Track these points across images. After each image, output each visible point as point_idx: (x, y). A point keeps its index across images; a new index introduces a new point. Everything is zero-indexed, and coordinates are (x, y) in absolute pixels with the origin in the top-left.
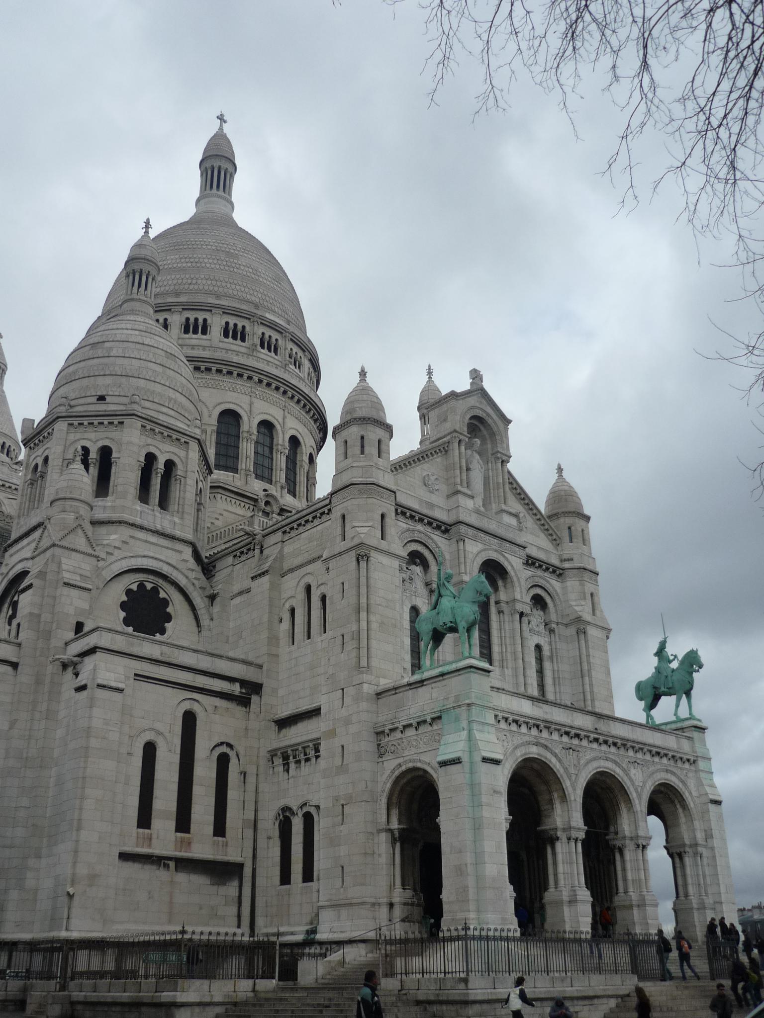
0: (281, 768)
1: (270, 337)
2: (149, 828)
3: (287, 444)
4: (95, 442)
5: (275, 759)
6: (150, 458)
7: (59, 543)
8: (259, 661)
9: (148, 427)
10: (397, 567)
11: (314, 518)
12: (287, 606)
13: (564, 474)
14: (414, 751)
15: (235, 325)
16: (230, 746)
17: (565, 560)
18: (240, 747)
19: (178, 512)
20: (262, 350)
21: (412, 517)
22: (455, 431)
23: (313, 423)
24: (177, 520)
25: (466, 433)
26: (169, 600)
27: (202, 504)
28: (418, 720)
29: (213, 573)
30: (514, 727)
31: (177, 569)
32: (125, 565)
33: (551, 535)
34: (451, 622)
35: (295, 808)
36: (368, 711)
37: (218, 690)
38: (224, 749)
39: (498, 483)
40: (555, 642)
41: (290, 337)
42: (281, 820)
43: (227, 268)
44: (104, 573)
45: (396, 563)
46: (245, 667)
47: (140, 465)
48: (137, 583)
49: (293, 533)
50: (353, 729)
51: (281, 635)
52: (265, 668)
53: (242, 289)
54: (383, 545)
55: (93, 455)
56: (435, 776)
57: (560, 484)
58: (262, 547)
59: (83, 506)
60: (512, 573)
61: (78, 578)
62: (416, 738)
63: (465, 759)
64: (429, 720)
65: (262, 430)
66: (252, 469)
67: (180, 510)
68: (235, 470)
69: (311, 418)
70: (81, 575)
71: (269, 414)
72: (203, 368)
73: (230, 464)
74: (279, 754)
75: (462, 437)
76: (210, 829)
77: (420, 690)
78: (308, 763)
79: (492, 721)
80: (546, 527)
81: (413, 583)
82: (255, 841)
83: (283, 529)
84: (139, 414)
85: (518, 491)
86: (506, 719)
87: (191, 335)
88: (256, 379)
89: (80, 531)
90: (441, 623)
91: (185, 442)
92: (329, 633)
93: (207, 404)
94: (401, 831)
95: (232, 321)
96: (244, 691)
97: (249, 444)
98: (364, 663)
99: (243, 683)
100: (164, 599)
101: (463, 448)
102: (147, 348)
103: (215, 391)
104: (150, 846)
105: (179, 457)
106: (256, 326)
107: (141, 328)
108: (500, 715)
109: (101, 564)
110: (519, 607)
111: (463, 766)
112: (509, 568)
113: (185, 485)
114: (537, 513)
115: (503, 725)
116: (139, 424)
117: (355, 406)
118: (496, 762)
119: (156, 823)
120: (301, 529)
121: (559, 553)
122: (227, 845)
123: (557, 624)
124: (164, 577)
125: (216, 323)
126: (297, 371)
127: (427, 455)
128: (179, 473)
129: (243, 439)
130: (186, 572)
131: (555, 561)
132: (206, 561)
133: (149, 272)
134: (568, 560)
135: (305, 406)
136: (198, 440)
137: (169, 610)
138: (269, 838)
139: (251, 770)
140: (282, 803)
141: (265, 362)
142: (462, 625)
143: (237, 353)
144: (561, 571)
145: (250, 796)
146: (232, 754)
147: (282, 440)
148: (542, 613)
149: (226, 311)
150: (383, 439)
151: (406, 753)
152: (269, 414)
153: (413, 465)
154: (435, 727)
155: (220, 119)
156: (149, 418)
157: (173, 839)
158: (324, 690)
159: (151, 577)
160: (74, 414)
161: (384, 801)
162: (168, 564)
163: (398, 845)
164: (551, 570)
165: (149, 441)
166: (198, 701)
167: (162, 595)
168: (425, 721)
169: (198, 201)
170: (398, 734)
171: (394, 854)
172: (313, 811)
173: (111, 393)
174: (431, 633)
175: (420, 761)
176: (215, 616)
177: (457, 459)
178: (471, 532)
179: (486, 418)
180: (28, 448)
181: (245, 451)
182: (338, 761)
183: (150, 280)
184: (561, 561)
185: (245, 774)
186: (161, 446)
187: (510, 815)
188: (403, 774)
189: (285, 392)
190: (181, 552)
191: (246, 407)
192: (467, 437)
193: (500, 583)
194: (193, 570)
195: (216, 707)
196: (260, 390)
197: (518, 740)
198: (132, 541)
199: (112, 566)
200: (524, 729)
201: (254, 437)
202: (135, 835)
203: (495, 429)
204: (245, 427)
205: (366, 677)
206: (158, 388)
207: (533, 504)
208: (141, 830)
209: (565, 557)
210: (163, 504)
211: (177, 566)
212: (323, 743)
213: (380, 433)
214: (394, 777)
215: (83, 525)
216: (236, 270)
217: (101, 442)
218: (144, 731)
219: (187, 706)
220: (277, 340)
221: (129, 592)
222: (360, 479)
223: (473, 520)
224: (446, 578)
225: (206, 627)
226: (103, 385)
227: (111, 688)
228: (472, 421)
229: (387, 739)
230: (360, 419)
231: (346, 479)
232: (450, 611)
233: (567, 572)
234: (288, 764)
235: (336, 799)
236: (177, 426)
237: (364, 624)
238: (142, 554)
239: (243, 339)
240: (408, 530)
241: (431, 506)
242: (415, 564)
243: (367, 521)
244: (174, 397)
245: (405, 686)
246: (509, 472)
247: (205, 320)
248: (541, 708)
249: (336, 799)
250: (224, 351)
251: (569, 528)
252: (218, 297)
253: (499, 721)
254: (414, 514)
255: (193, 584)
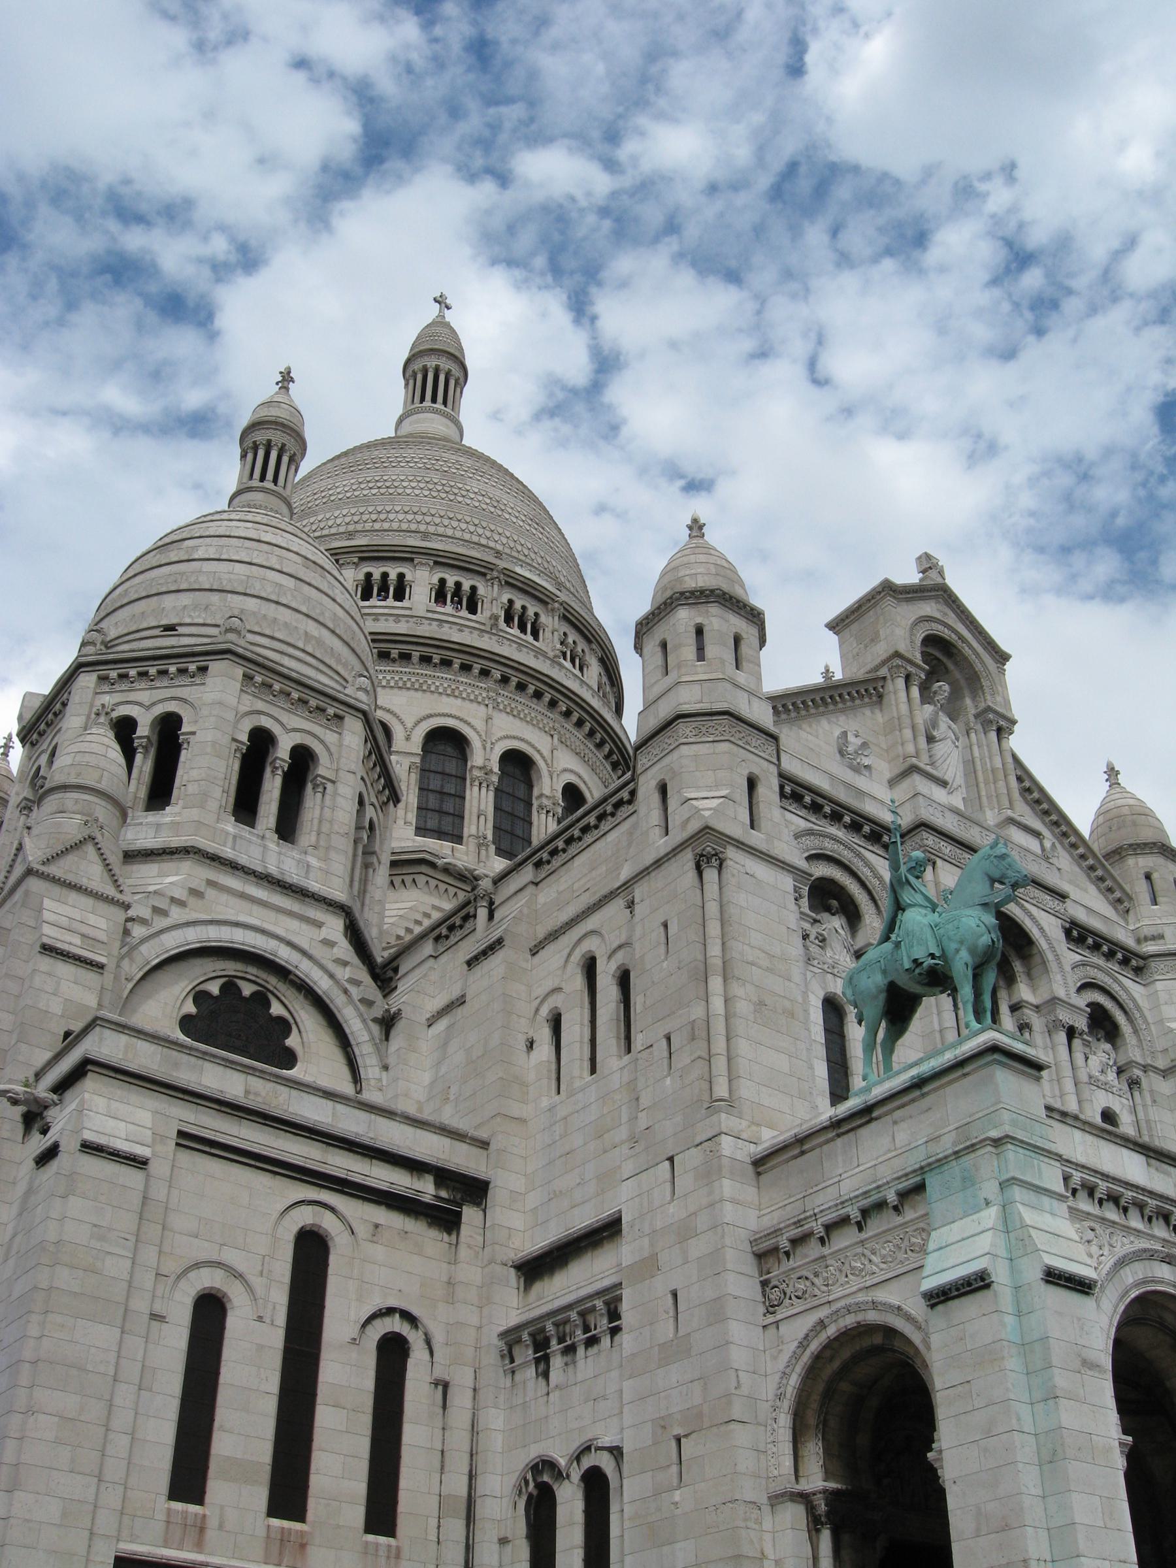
0: (531, 1372)
1: (524, 608)
2: (200, 1501)
3: (559, 795)
4: (148, 708)
5: (517, 1351)
6: (261, 741)
7: (42, 868)
8: (483, 1134)
9: (258, 679)
10: (791, 889)
11: (601, 818)
12: (545, 1011)
13: (1121, 779)
14: (855, 1283)
15: (458, 585)
16: (409, 1317)
17: (1146, 939)
18: (435, 1321)
19: (315, 847)
20: (508, 630)
21: (816, 808)
22: (897, 654)
23: (609, 768)
24: (313, 861)
25: (921, 663)
26: (291, 1021)
27: (374, 853)
28: (865, 1203)
29: (393, 985)
30: (1112, 1214)
31: (310, 957)
32: (193, 937)
33: (1110, 890)
34: (932, 956)
35: (562, 1462)
36: (734, 1201)
37: (383, 1186)
38: (395, 1324)
39: (993, 771)
40: (1145, 1106)
41: (562, 610)
42: (530, 1496)
43: (444, 495)
44: (144, 948)
45: (787, 882)
46: (446, 1141)
47: (234, 745)
48: (222, 981)
49: (556, 862)
50: (698, 1248)
51: (531, 1077)
52: (493, 1147)
53: (472, 528)
54: (756, 839)
55: (143, 730)
56: (916, 1338)
57: (1117, 796)
58: (491, 903)
59: (103, 803)
60: (1043, 944)
61: (77, 940)
62: (860, 1250)
63: (1000, 1275)
64: (892, 1197)
65: (510, 769)
66: (490, 837)
67: (322, 843)
68: (458, 838)
69: (607, 757)
70: (83, 936)
71: (522, 740)
72: (394, 654)
73: (448, 828)
74: (525, 1336)
75: (911, 669)
76: (357, 1515)
77: (864, 1132)
78: (593, 1350)
79: (1059, 1187)
80: (1100, 873)
81: (828, 950)
82: (469, 1548)
83: (536, 858)
84: (240, 651)
85: (1036, 795)
86: (1091, 1191)
87: (374, 601)
88: (497, 675)
89: (90, 849)
90: (907, 965)
91: (336, 716)
92: (638, 1041)
93: (403, 716)
94: (833, 1497)
95: (451, 579)
96: (444, 1194)
97: (484, 790)
98: (721, 1090)
99: (443, 1176)
100: (281, 1020)
101: (915, 692)
102: (265, 547)
103: (420, 694)
104: (199, 1546)
105: (322, 742)
106: (496, 587)
107: (259, 518)
108: (1077, 1177)
109: (138, 931)
110: (1065, 1016)
111: (996, 1295)
112: (1035, 933)
113: (335, 793)
114: (1079, 843)
115: (1085, 1205)
116: (239, 672)
117: (680, 574)
118: (1081, 1286)
119: (216, 1488)
120: (573, 849)
121: (1132, 927)
122: (398, 1556)
123: (1145, 1068)
124: (282, 972)
125: (422, 580)
126: (577, 672)
127: (840, 696)
128: (321, 771)
129: (472, 781)
130: (331, 966)
131: (1123, 936)
132: (379, 960)
133: (284, 445)
134: (1153, 938)
135: (591, 734)
136: (364, 713)
137: (292, 1041)
138: (503, 1541)
139: (462, 1379)
140: (534, 1452)
141: (515, 646)
142: (961, 965)
143: (461, 628)
144: (1141, 963)
145: (459, 1440)
146: (415, 1339)
147: (548, 787)
148: (1108, 1046)
149: (441, 560)
150: (744, 636)
151: (837, 1292)
152: (522, 740)
153: (813, 711)
154: (909, 1214)
155: (439, 302)
156: (260, 660)
157: (261, 1532)
158: (628, 1168)
159: (252, 971)
160: (111, 657)
161: (785, 1421)
162: (290, 944)
163: (826, 1536)
164: (1119, 956)
165: (260, 705)
166: (332, 1209)
167: (276, 1009)
168: (881, 1205)
169: (400, 421)
170: (813, 1250)
171: (815, 1558)
172: (605, 1462)
173: (188, 620)
174: (883, 996)
175: (875, 1305)
176: (391, 1061)
177: (904, 708)
178: (947, 848)
179: (959, 644)
180: (28, 745)
181: (475, 803)
182: (666, 1330)
183: (285, 459)
184: (1139, 941)
185: (446, 1386)
186: (285, 717)
187: (1125, 1432)
188: (832, 1346)
189: (553, 704)
190: (319, 925)
191: (479, 724)
192: (923, 669)
193: (1018, 966)
194: (345, 964)
195: (377, 1226)
196: (506, 695)
197: (1125, 1245)
198: (211, 893)
199: (164, 937)
200: (1136, 1222)
201: (495, 779)
202: (161, 1516)
203: (978, 667)
204: (477, 758)
205: (726, 1121)
206: (284, 615)
207: (1069, 823)
208: (178, 1506)
209: (1147, 931)
210: (287, 829)
211: (312, 952)
212: (626, 1294)
213: (738, 624)
214: (806, 1357)
215: (99, 838)
216: (460, 499)
217: (160, 706)
218: (197, 1265)
219: (305, 1217)
220: (536, 614)
221: (200, 997)
222: (698, 706)
223: (949, 823)
224: (911, 870)
225: (373, 1082)
226: (172, 609)
227: (116, 1156)
228: (930, 650)
229: (786, 1265)
230: (692, 593)
231: (664, 711)
232: (928, 934)
233: (1153, 964)
234: (546, 1359)
235: (662, 1424)
236: (319, 682)
237: (718, 1004)
238: (233, 918)
239: (472, 609)
240: (810, 833)
241: (861, 793)
242: (828, 909)
243: (717, 786)
244: (316, 634)
245: (824, 1129)
246: (1015, 757)
247: (401, 576)
248: (1165, 1173)
249: (662, 1424)
250: (435, 623)
251: (1148, 877)
252: (426, 536)
253: (1074, 1192)
254: (820, 800)
255: (346, 991)
